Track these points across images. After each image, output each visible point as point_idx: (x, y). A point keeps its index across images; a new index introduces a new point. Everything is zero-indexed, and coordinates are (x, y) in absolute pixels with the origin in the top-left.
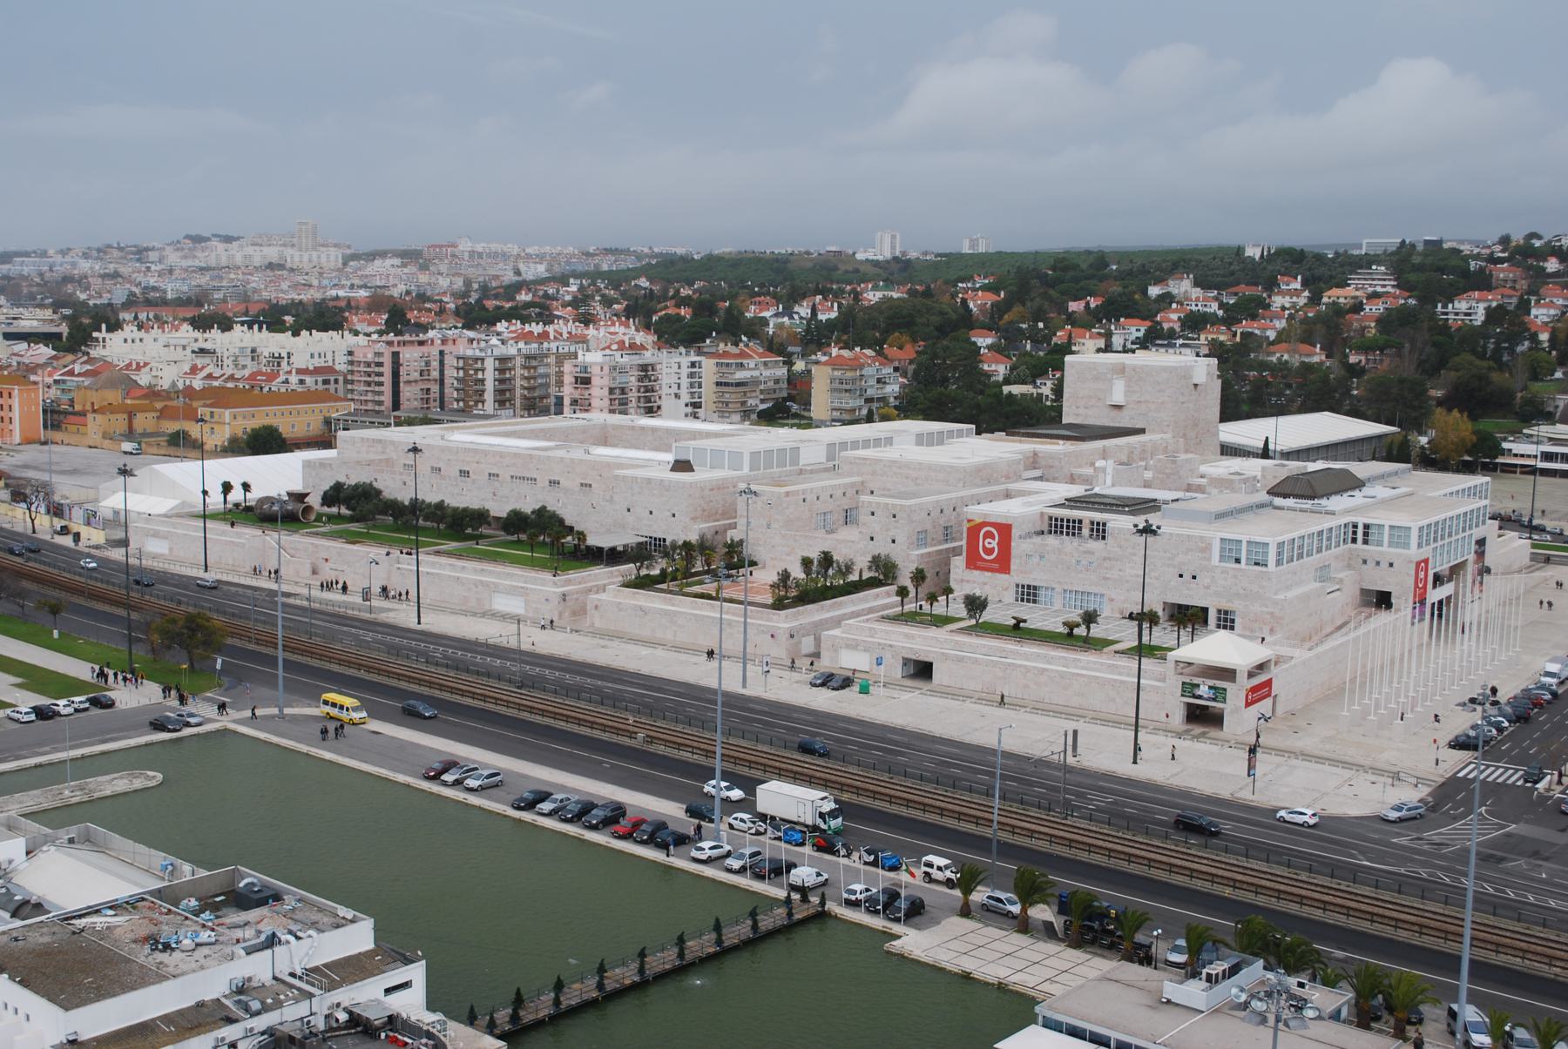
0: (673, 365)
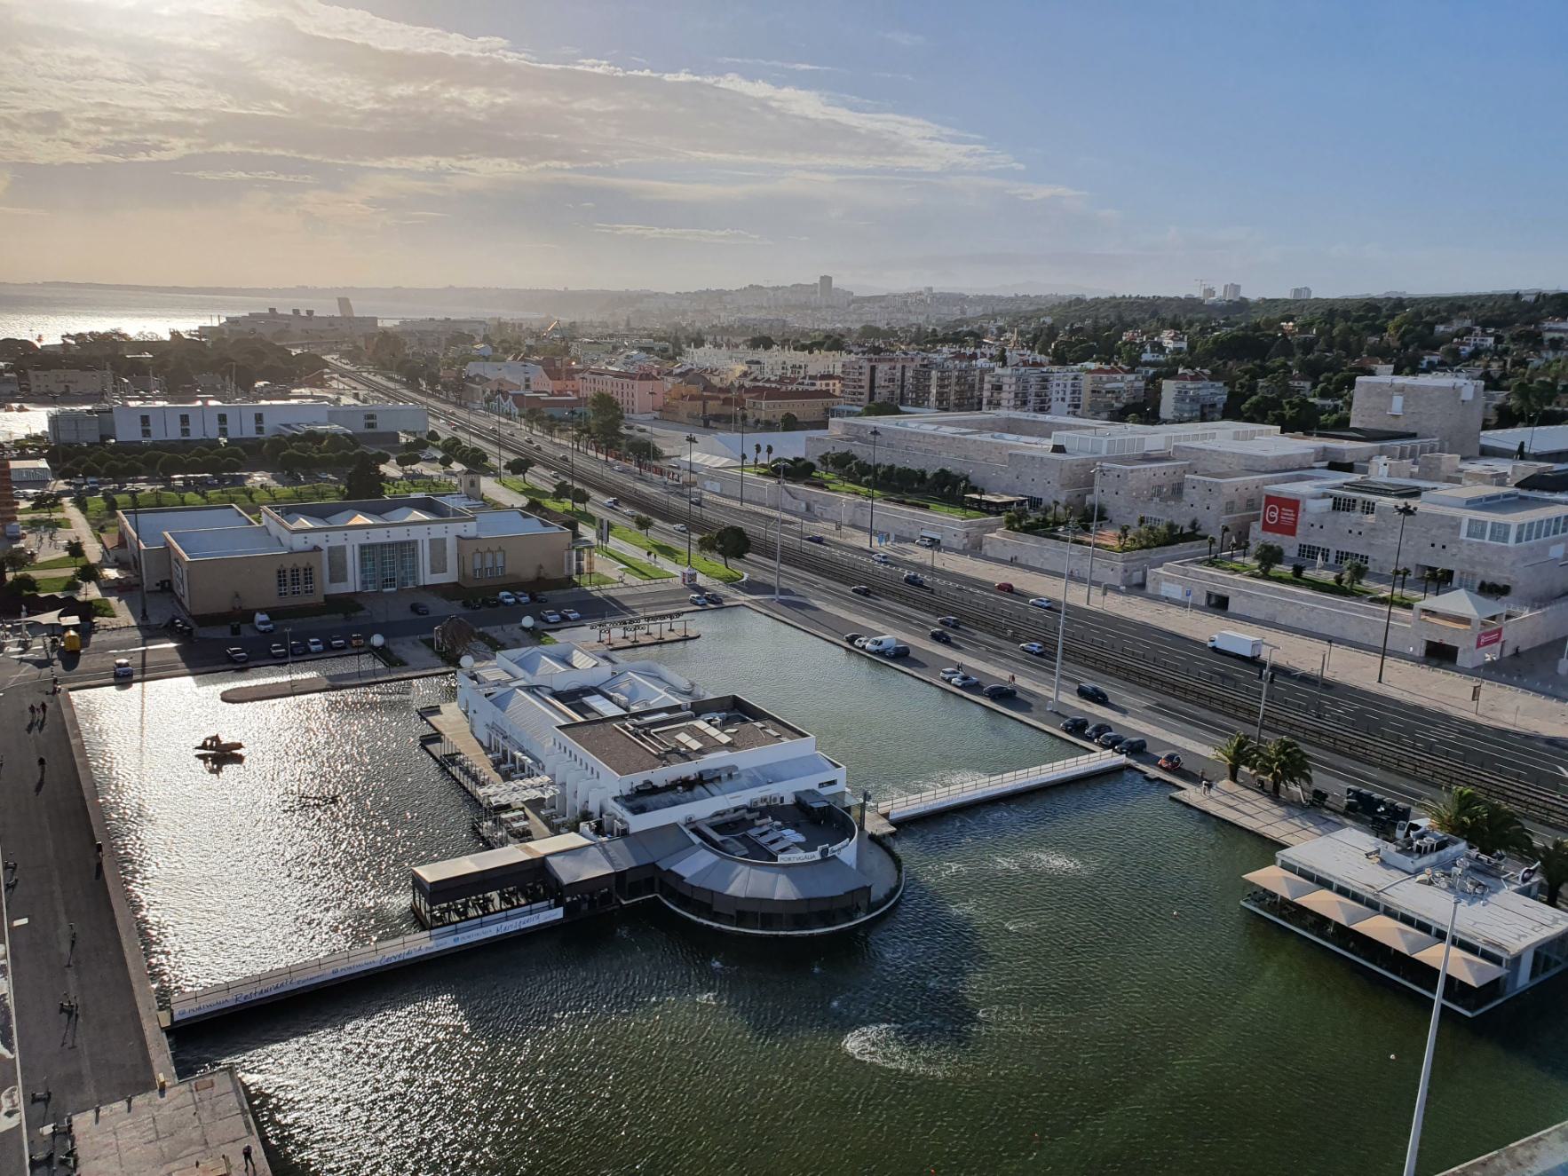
0: (1061, 377)
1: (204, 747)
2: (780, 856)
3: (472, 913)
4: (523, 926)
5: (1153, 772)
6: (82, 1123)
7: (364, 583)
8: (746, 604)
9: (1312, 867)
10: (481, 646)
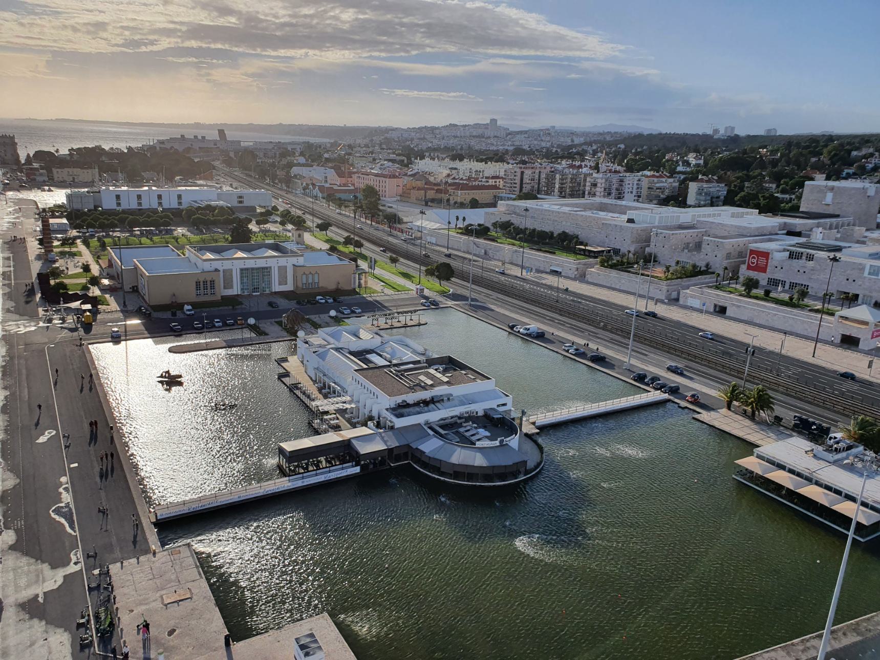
0: (631, 179)
1: (161, 376)
2: (477, 443)
3: (311, 468)
4: (338, 476)
5: (683, 404)
6: (114, 568)
7: (242, 289)
8: (452, 306)
9: (774, 458)
10: (308, 325)
